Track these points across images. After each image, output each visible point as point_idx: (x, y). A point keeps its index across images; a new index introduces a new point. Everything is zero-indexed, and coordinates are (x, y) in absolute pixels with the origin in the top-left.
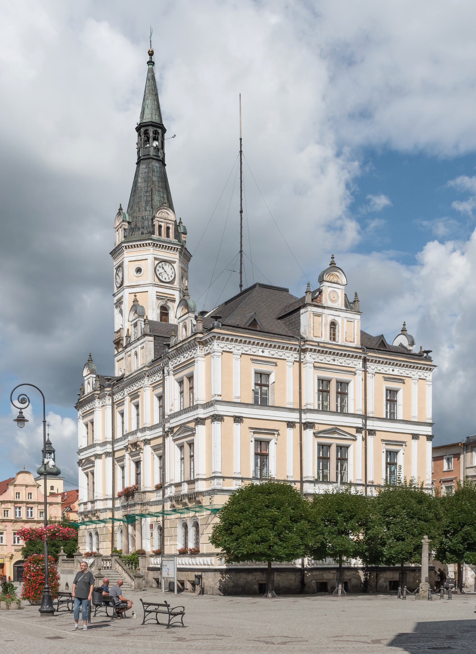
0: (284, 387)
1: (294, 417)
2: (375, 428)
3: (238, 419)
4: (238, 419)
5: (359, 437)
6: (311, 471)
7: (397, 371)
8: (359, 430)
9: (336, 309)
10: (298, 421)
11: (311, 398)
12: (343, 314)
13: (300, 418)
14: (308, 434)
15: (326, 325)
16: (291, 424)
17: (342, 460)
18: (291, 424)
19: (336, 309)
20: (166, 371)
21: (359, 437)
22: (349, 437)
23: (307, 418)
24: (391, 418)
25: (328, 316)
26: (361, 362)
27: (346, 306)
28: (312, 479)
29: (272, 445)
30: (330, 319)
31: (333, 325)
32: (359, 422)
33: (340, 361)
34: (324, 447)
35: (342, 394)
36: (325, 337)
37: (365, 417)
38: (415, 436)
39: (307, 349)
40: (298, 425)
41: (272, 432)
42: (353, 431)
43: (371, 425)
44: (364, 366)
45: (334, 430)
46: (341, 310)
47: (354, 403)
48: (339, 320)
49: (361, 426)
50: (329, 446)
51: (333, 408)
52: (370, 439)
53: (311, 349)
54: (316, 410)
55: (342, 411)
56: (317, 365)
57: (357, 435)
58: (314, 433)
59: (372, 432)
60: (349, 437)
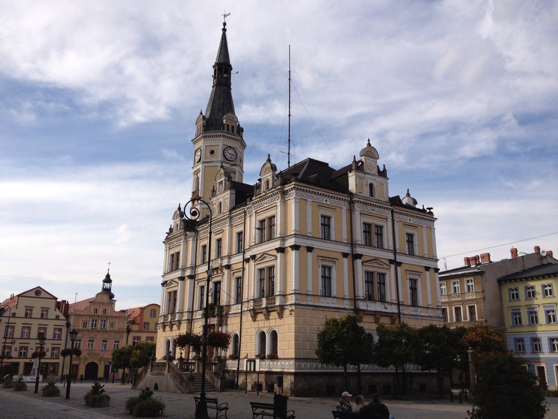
0: (339, 228)
1: (347, 250)
2: (401, 261)
5: (393, 267)
6: (361, 292)
7: (412, 221)
8: (391, 262)
9: (373, 175)
10: (350, 253)
11: (359, 236)
14: (359, 262)
15: (366, 185)
16: (345, 255)
17: (382, 283)
18: (345, 255)
19: (373, 175)
20: (248, 215)
21: (393, 267)
24: (411, 253)
26: (390, 212)
27: (378, 173)
28: (363, 298)
29: (334, 271)
30: (369, 181)
31: (371, 185)
32: (391, 256)
33: (376, 211)
34: (369, 275)
35: (380, 235)
36: (366, 192)
37: (395, 252)
38: (427, 269)
39: (356, 200)
40: (350, 257)
43: (399, 258)
44: (392, 216)
47: (388, 242)
49: (393, 258)
50: (372, 273)
52: (399, 269)
53: (358, 201)
55: (380, 247)
56: (362, 212)
58: (362, 263)
59: (399, 264)
60: (386, 266)
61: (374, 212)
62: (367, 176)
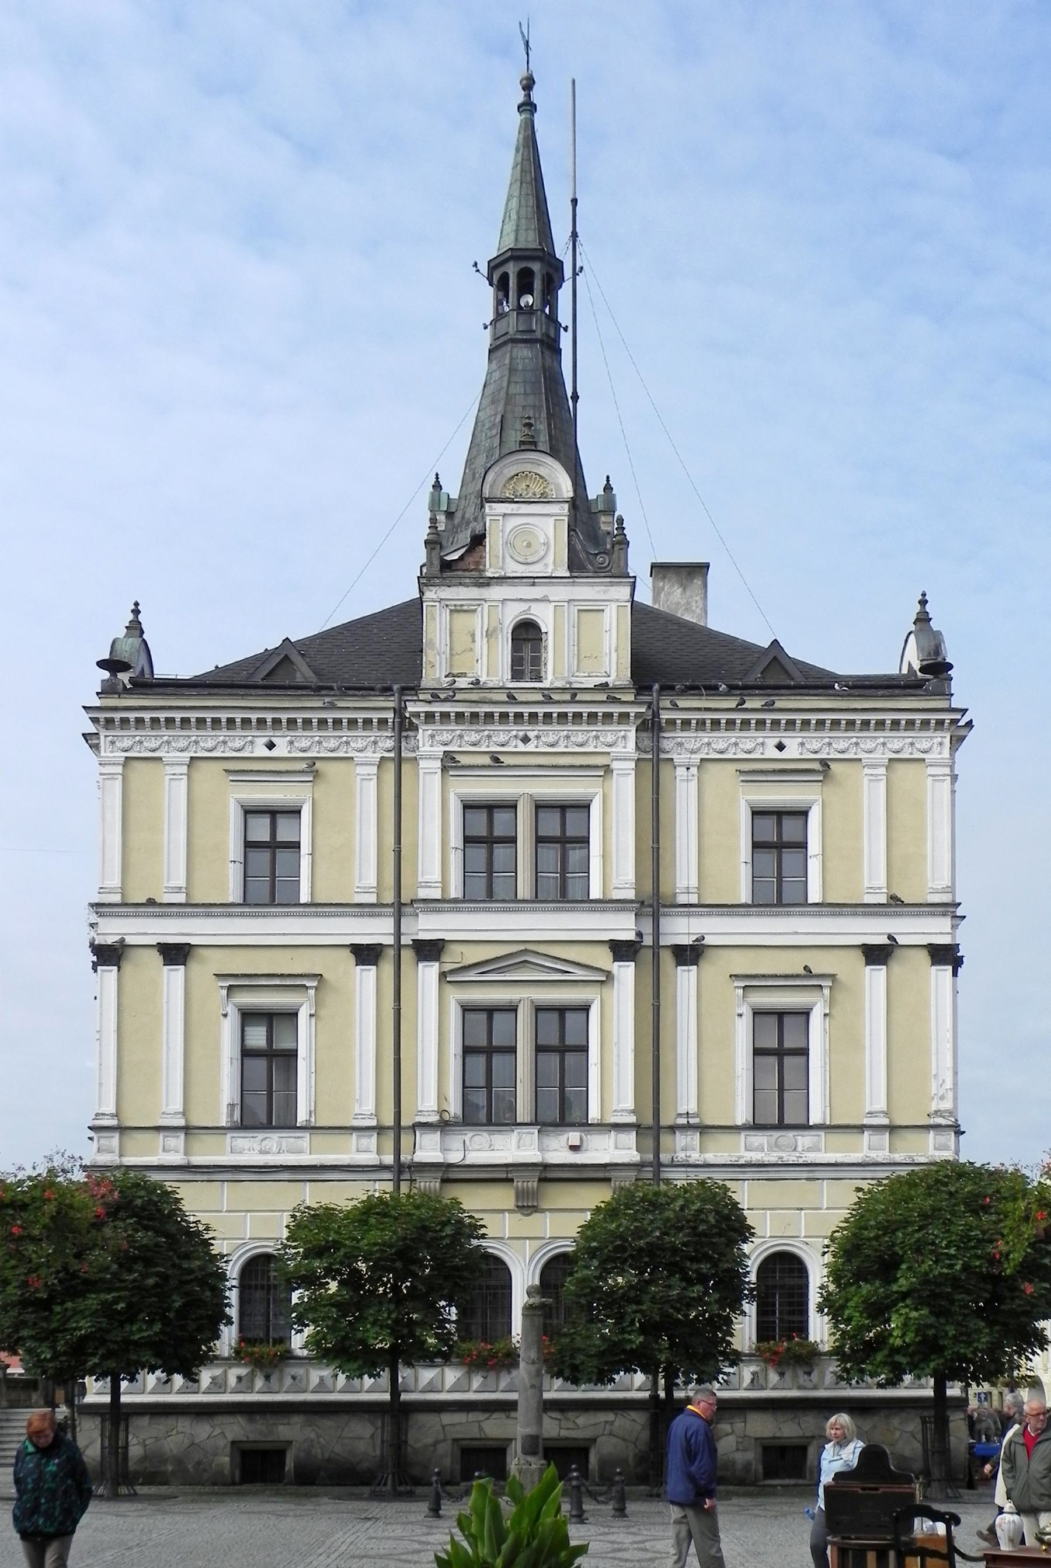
1: (377, 930)
3: (175, 954)
4: (175, 954)
8: (622, 950)
12: (561, 592)
13: (398, 934)
22: (580, 974)
23: (426, 926)
25: (507, 607)
30: (512, 615)
31: (527, 633)
32: (624, 926)
33: (547, 739)
41: (293, 982)
42: (603, 958)
45: (521, 956)
46: (551, 579)
48: (545, 617)
49: (631, 936)
51: (524, 889)
54: (455, 901)
57: (616, 967)
58: (443, 975)
60: (580, 974)
61: (530, 747)
62: (496, 592)
